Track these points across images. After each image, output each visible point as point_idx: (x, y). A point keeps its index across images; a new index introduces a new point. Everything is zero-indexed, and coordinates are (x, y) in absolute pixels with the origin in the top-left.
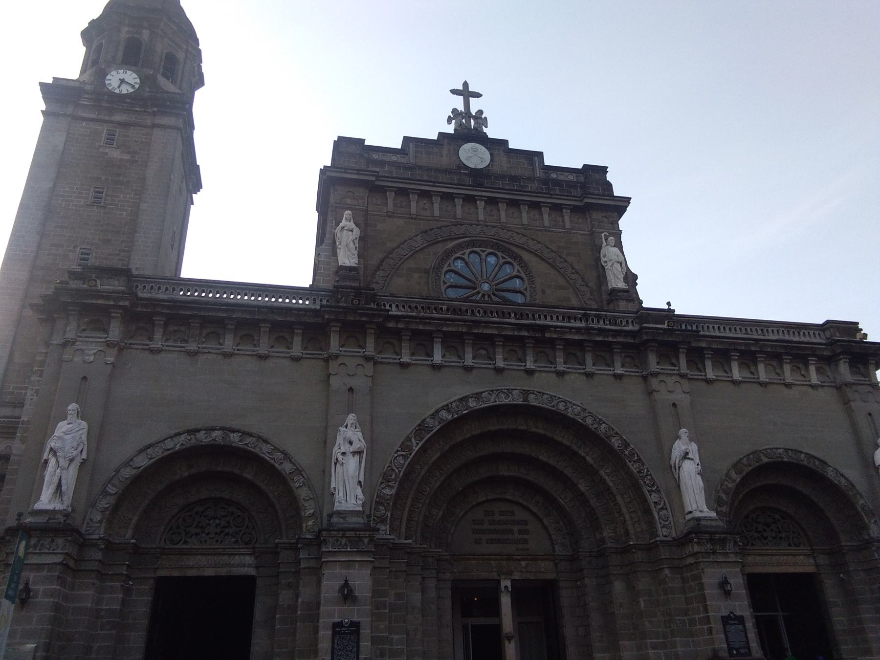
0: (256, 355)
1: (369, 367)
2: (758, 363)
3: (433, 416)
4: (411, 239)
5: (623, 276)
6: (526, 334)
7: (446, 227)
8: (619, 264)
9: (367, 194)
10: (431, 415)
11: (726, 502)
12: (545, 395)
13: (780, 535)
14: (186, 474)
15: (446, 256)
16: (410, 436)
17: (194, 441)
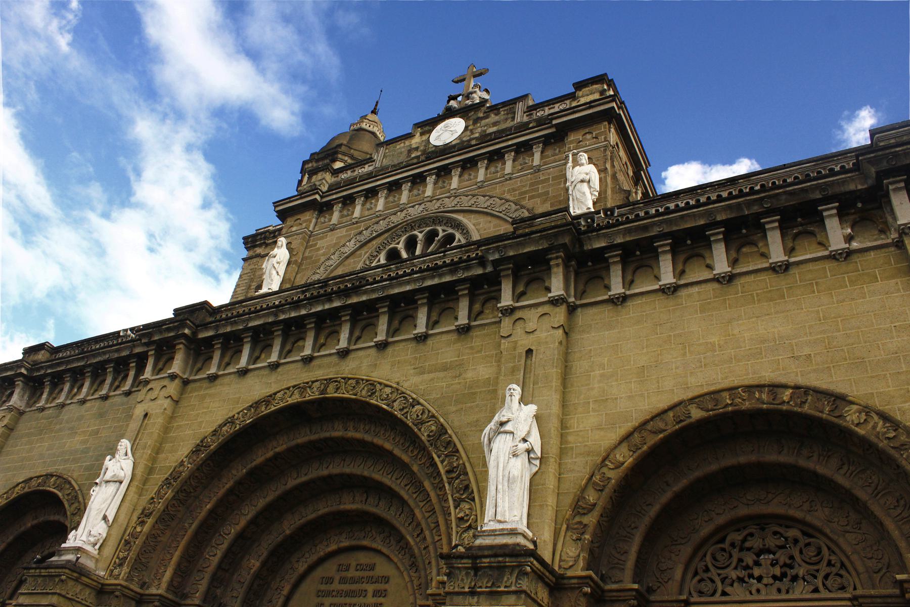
0: (100, 398)
1: (173, 388)
2: (714, 246)
3: (215, 433)
4: (344, 246)
5: (593, 197)
6: (336, 304)
7: (384, 219)
8: (585, 184)
9: (315, 215)
10: (213, 432)
11: (594, 505)
12: (350, 381)
13: (793, 572)
14: (29, 525)
15: (377, 252)
16: (185, 460)
17: (26, 490)
